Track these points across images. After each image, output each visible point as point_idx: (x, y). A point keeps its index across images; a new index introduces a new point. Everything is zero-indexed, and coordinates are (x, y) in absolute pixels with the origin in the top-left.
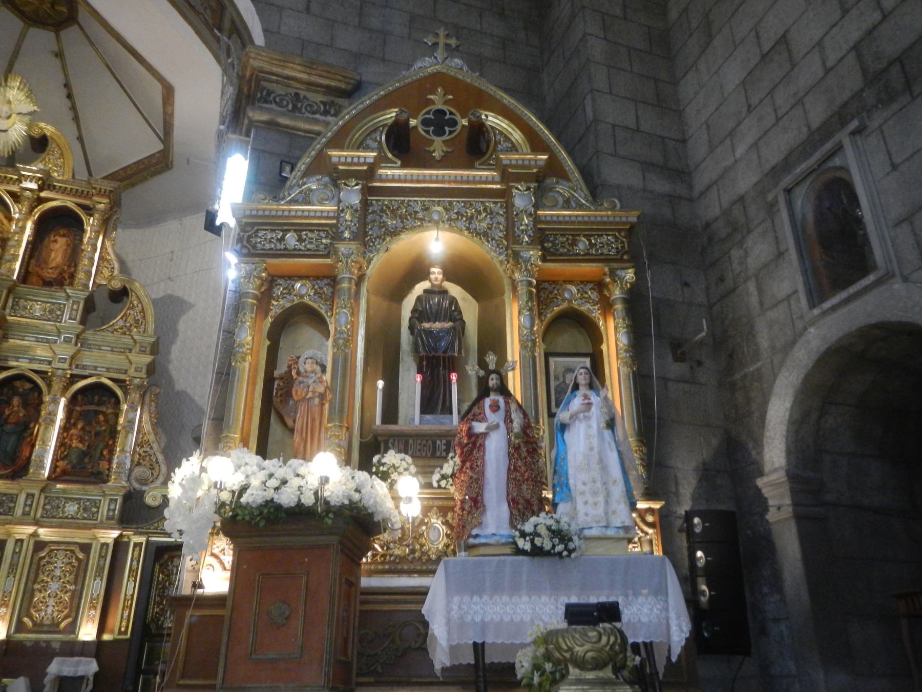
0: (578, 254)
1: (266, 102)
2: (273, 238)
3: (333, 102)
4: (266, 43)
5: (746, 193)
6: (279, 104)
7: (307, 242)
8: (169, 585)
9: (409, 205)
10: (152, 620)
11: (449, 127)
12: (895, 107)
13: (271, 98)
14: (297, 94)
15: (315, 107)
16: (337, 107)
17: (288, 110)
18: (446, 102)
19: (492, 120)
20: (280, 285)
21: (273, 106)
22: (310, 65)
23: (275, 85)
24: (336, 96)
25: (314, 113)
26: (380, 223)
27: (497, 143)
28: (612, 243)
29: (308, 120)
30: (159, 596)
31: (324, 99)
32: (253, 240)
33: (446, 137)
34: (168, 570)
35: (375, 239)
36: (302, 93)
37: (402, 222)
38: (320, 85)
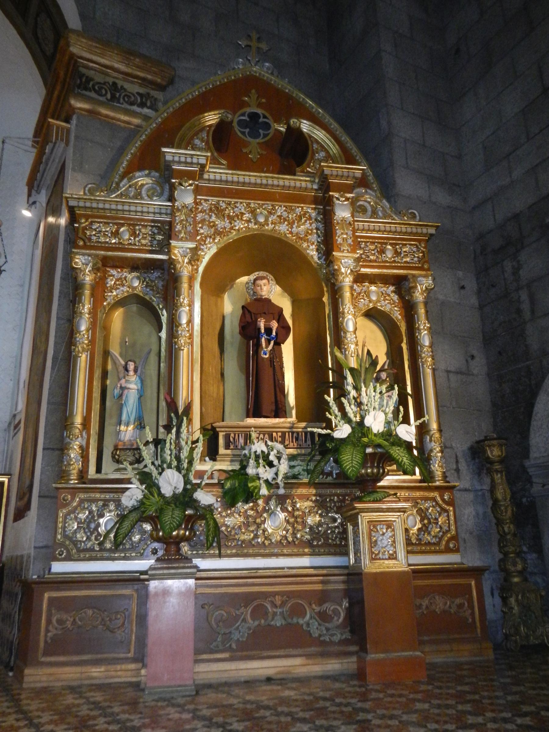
1: (86, 89)
2: (107, 231)
5: (521, 212)
7: (140, 237)
9: (236, 207)
11: (263, 130)
13: (91, 85)
14: (114, 84)
15: (133, 99)
16: (153, 99)
17: (107, 99)
18: (260, 105)
19: (305, 126)
20: (113, 276)
21: (93, 95)
23: (92, 72)
25: (132, 104)
26: (210, 222)
28: (414, 252)
29: (127, 112)
32: (88, 233)
35: (206, 237)
36: (120, 83)
38: (137, 77)
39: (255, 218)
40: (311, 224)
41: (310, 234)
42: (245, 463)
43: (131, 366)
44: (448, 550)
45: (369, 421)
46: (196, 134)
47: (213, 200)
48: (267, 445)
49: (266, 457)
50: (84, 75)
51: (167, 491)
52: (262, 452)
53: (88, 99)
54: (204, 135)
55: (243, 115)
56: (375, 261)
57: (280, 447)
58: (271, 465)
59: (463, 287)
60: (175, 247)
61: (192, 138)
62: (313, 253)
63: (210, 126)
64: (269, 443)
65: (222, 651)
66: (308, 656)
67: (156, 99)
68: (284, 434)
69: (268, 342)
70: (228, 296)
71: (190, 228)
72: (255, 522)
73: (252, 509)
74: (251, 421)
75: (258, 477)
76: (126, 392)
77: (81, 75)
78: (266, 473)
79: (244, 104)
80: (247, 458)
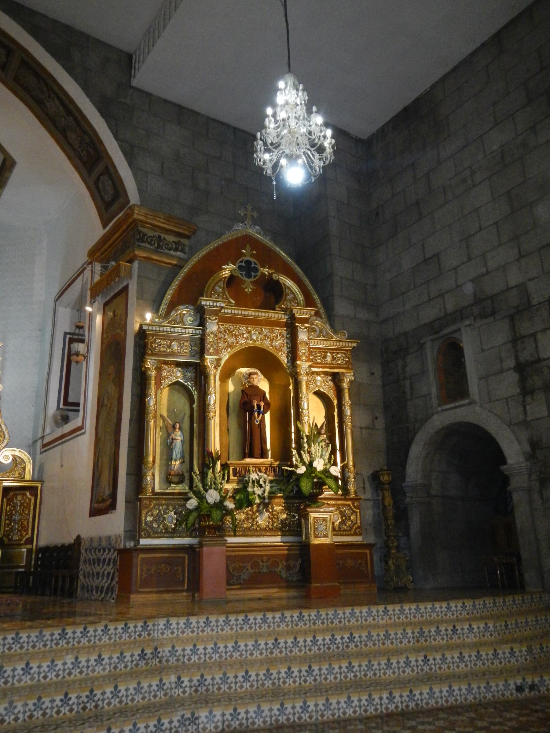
0: (327, 364)
1: (143, 242)
3: (179, 241)
4: (141, 201)
6: (150, 243)
8: (16, 512)
10: (4, 535)
12: (486, 321)
13: (145, 239)
14: (160, 236)
18: (252, 256)
20: (166, 369)
21: (147, 245)
22: (169, 219)
23: (146, 229)
24: (182, 238)
25: (170, 249)
26: (225, 339)
27: (287, 295)
29: (168, 255)
30: (8, 519)
31: (176, 239)
32: (154, 345)
33: (252, 279)
34: (13, 503)
36: (163, 236)
37: (237, 340)
38: (174, 232)
39: (251, 336)
40: (283, 340)
41: (283, 347)
42: (246, 485)
43: (178, 426)
44: (355, 534)
45: (315, 464)
46: (217, 283)
47: (227, 325)
48: (258, 475)
49: (258, 482)
50: (141, 232)
51: (211, 500)
52: (256, 479)
53: (145, 249)
54: (222, 283)
55: (242, 262)
56: (320, 363)
57: (265, 476)
58: (261, 486)
59: (373, 374)
60: (207, 359)
61: (214, 286)
62: (284, 358)
63: (225, 278)
64: (260, 474)
65: (236, 585)
66: (279, 587)
67: (184, 245)
68: (266, 469)
69: (259, 414)
70: (232, 381)
71: (215, 347)
72: (252, 518)
73: (250, 511)
74: (248, 460)
75: (254, 493)
76: (175, 441)
77: (140, 232)
78: (258, 491)
79: (243, 255)
80: (247, 483)
